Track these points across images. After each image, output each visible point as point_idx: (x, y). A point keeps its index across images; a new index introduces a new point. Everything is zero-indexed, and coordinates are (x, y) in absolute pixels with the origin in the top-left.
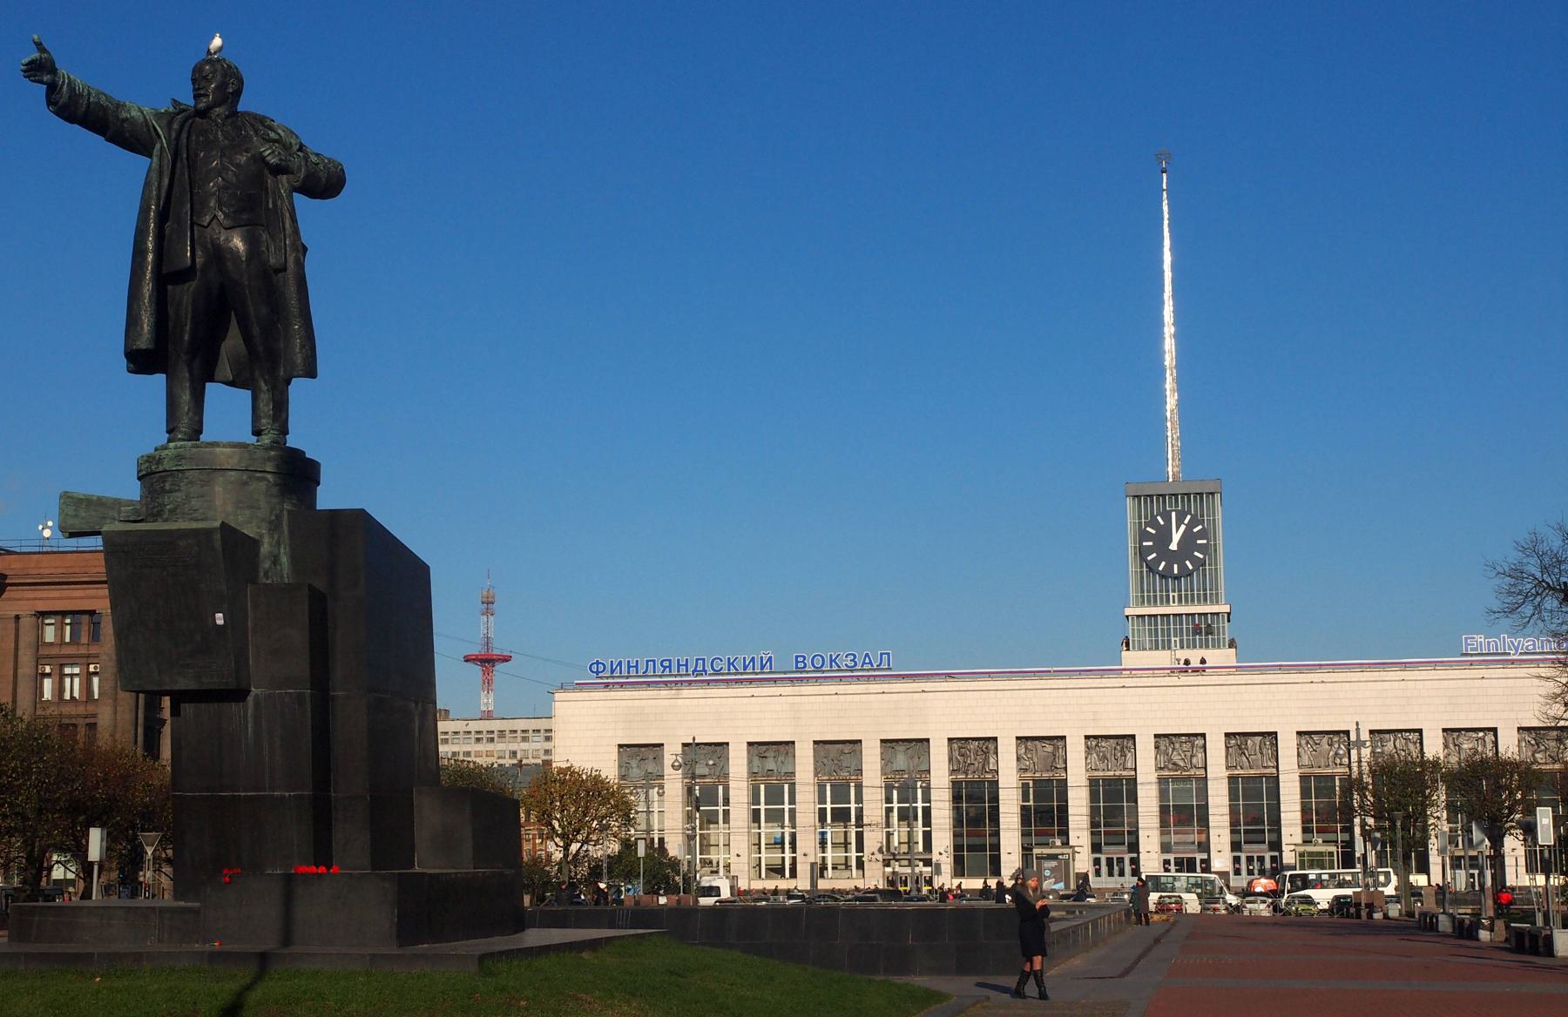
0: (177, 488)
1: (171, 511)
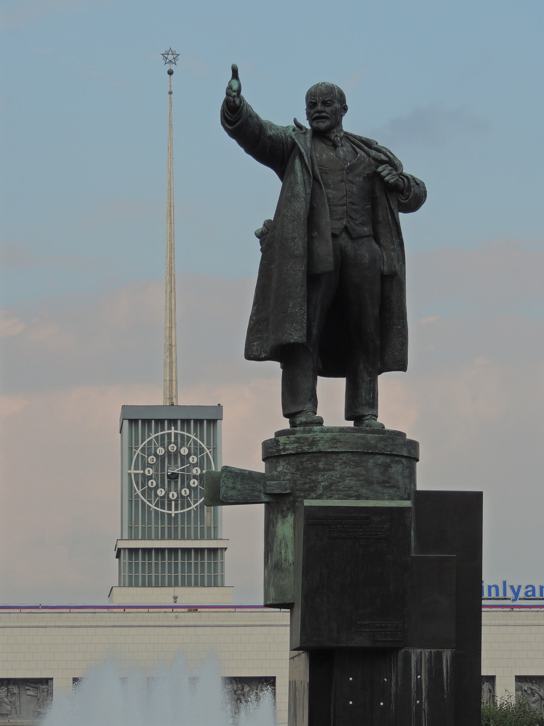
0: (331, 468)
1: (325, 488)
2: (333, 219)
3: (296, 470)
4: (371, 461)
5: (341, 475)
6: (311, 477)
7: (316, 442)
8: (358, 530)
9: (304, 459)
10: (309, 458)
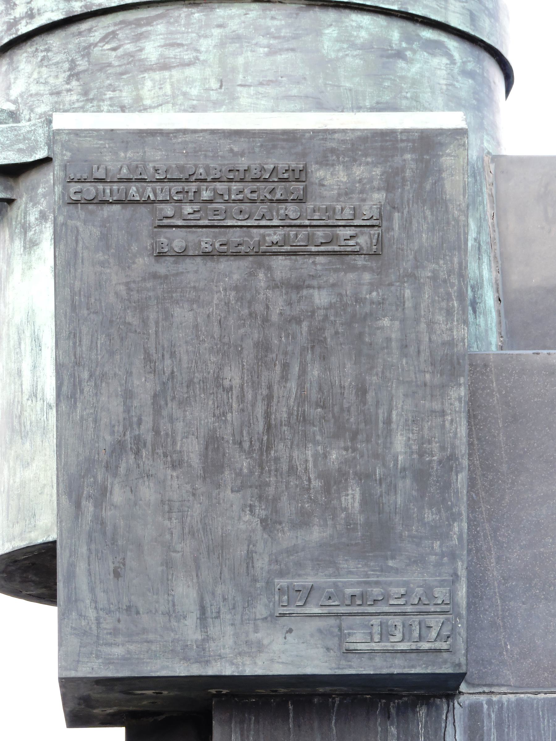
0: (187, 56)
3: (69, 76)
4: (331, 32)
5: (221, 81)
6: (117, 93)
8: (263, 223)
9: (97, 35)
10: (111, 29)
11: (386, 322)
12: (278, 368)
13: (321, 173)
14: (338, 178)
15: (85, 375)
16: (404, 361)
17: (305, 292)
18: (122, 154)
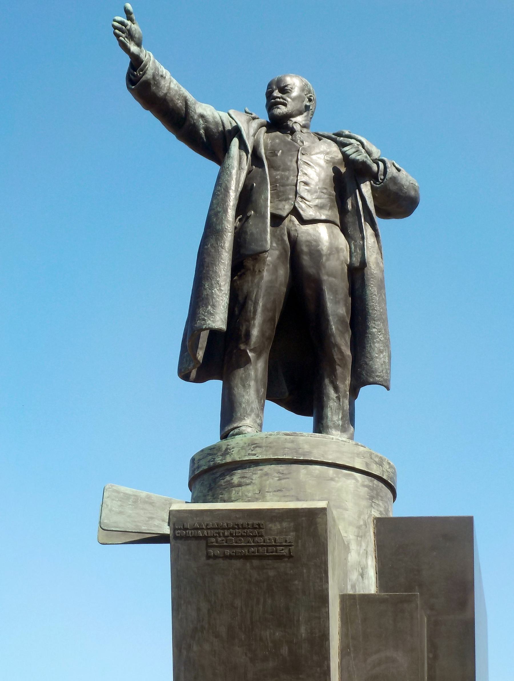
0: (248, 481)
2: (279, 200)
7: (230, 450)
11: (296, 582)
12: (255, 600)
13: (270, 525)
14: (277, 527)
15: (182, 602)
16: (304, 597)
17: (265, 571)
18: (195, 519)
